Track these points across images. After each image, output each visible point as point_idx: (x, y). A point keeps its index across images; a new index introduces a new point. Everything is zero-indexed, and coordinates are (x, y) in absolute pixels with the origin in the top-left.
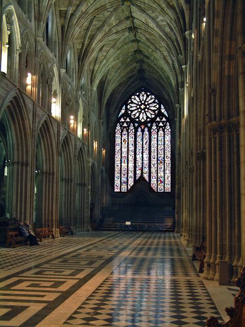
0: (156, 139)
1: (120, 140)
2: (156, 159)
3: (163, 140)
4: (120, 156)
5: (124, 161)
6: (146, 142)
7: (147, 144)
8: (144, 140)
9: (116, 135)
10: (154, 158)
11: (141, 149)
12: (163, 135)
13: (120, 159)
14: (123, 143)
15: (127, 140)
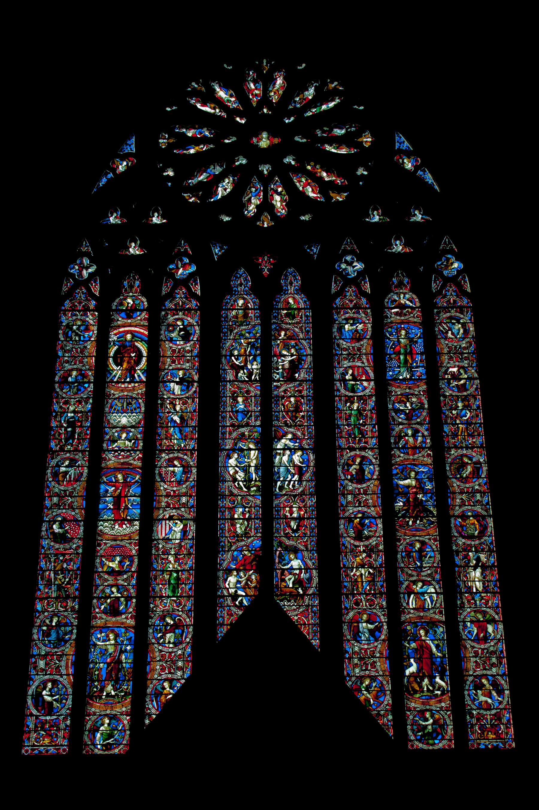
0: (366, 345)
1: (91, 347)
2: (373, 485)
3: (419, 347)
4: (82, 461)
5: (118, 500)
6: (295, 366)
7: (301, 375)
8: (277, 346)
9: (64, 320)
10: (360, 477)
11: (255, 408)
12: (416, 317)
13: (80, 487)
14: (117, 371)
15: (143, 348)
